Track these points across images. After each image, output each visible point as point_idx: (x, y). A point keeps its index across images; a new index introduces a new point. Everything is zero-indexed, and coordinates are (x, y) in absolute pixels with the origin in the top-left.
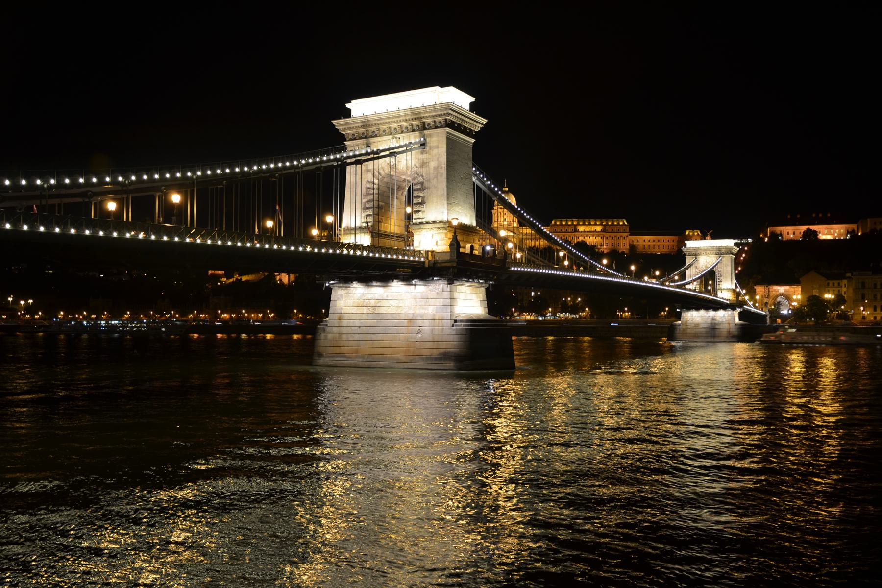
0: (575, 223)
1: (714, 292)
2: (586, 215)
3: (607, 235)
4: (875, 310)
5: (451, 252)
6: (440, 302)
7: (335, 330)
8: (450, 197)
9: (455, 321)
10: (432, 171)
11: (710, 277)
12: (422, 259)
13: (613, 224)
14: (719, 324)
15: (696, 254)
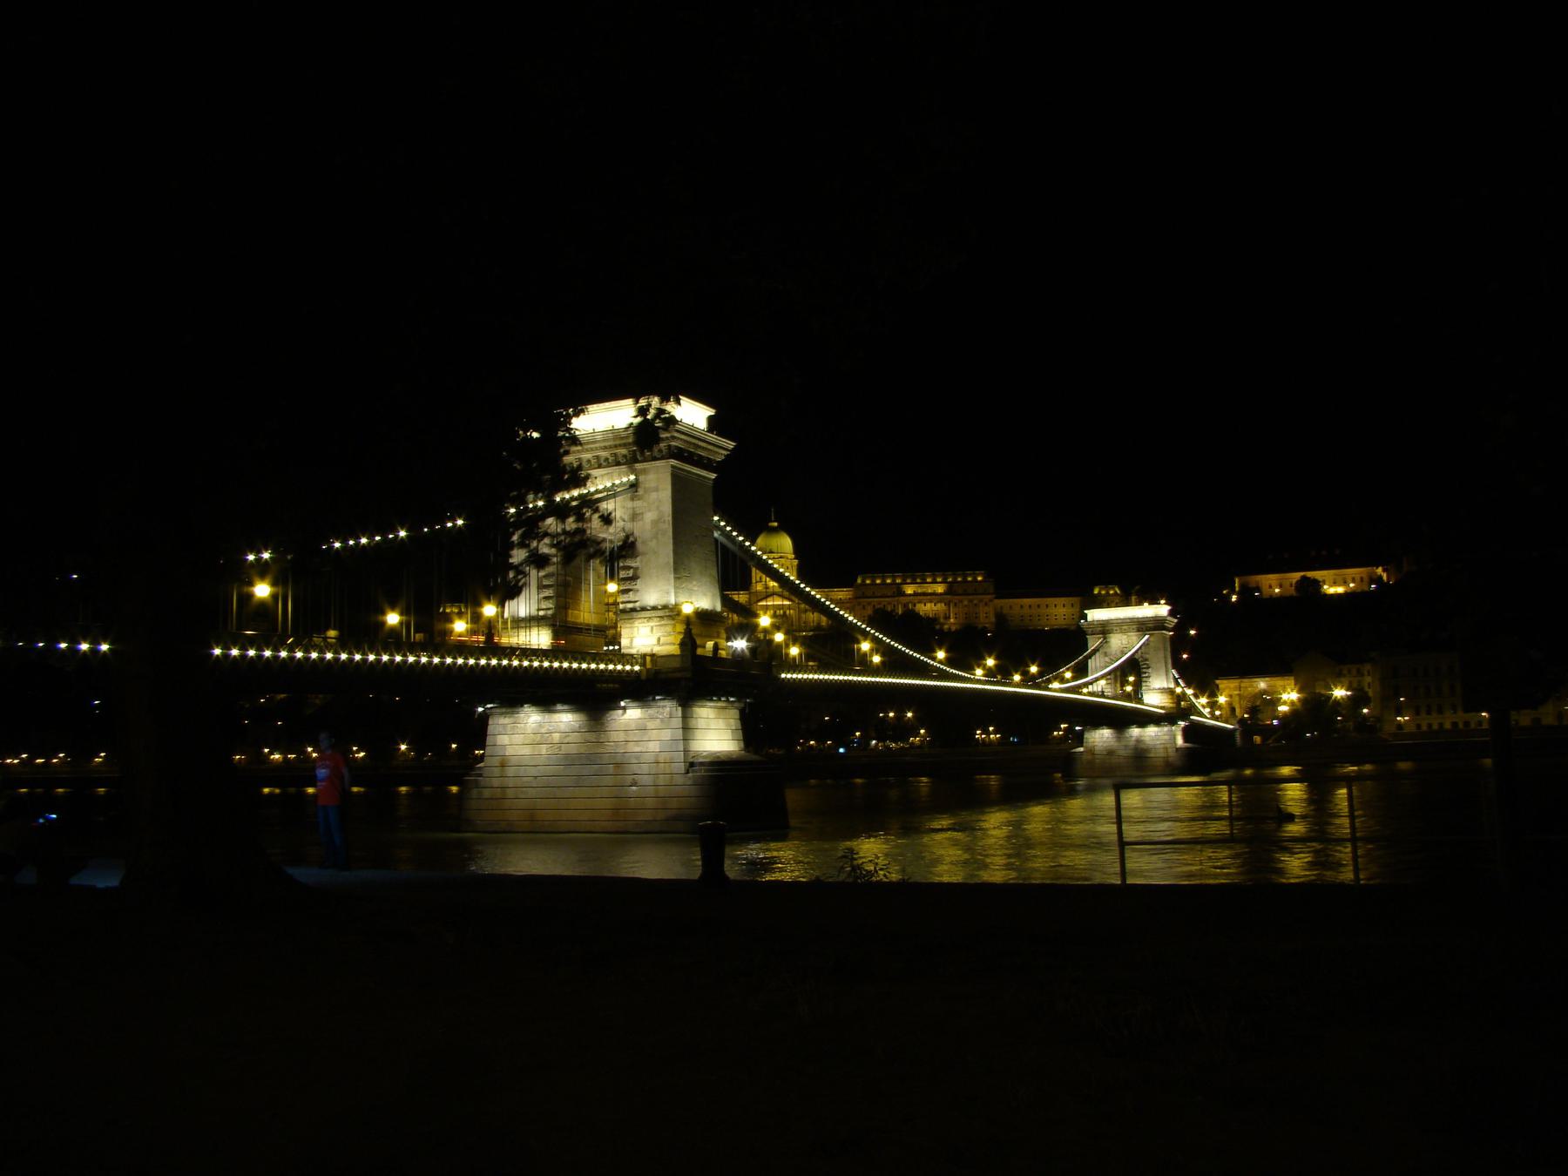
1: (1136, 696)
2: (917, 567)
4: (1418, 713)
5: (681, 656)
6: (666, 735)
7: (496, 782)
8: (681, 569)
9: (692, 765)
10: (648, 526)
12: (637, 668)
15: (1105, 629)
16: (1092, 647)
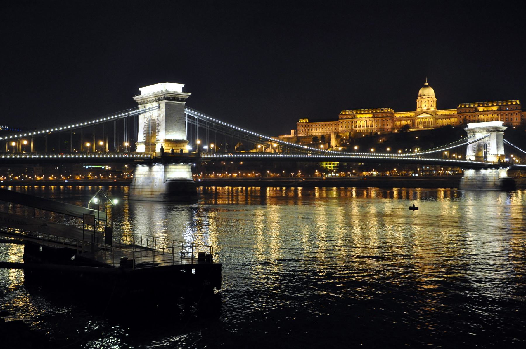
0: (476, 106)
3: (502, 112)
8: (167, 129)
11: (481, 147)
13: (507, 105)
14: (487, 178)
15: (474, 131)
16: (468, 136)
